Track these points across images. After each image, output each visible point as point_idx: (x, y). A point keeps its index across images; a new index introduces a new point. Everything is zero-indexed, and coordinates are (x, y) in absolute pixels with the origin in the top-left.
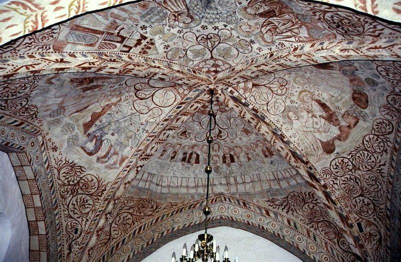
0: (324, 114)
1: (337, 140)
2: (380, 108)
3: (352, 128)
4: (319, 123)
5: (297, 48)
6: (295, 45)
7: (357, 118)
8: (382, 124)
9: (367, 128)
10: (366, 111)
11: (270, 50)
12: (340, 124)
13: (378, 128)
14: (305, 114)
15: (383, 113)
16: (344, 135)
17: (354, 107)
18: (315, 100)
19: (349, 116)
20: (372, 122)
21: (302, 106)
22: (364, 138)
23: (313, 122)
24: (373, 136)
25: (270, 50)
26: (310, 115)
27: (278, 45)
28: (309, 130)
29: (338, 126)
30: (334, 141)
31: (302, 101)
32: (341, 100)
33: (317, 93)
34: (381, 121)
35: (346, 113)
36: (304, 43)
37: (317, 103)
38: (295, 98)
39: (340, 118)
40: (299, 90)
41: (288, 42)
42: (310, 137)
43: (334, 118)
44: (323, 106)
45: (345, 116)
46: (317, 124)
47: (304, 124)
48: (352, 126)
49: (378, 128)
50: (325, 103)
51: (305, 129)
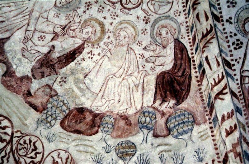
0: (56, 55)
1: (5, 69)
2: (66, 151)
3: (25, 98)
4: (40, 43)
5: (230, 68)
6: (237, 67)
7: (44, 109)
8: (33, 150)
9: (25, 125)
10: (57, 128)
11: (227, 21)
12: (35, 78)
13: (25, 142)
14: (64, 22)
15: (55, 155)
16: (13, 83)
17: (64, 108)
18: (83, 44)
19: (47, 97)
20: (37, 133)
21: (77, 20)
22: (6, 118)
23: (45, 32)
24: (10, 134)
25: (227, 21)
26: (58, 30)
27: (237, 37)
28: (33, 21)
29: (30, 75)
30: (4, 63)
31: (85, 22)
32: (80, 89)
33: (96, 51)
34: (40, 150)
35: (53, 93)
36: (239, 81)
37: (77, 45)
38: (94, 11)
39: (45, 80)
40: (107, 23)
41: (242, 57)
42: (19, 21)
43: (47, 71)
44: (71, 56)
45: (48, 90)
46: (41, 38)
47: (45, 15)
48: (31, 100)
49: (25, 142)
50: (76, 61)
51: (36, 14)
